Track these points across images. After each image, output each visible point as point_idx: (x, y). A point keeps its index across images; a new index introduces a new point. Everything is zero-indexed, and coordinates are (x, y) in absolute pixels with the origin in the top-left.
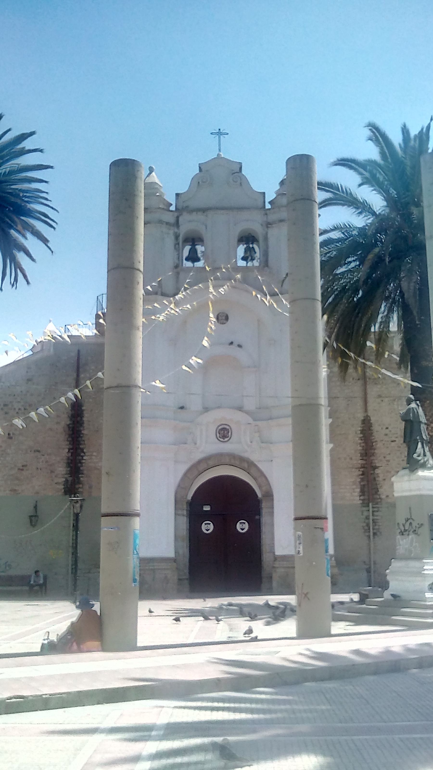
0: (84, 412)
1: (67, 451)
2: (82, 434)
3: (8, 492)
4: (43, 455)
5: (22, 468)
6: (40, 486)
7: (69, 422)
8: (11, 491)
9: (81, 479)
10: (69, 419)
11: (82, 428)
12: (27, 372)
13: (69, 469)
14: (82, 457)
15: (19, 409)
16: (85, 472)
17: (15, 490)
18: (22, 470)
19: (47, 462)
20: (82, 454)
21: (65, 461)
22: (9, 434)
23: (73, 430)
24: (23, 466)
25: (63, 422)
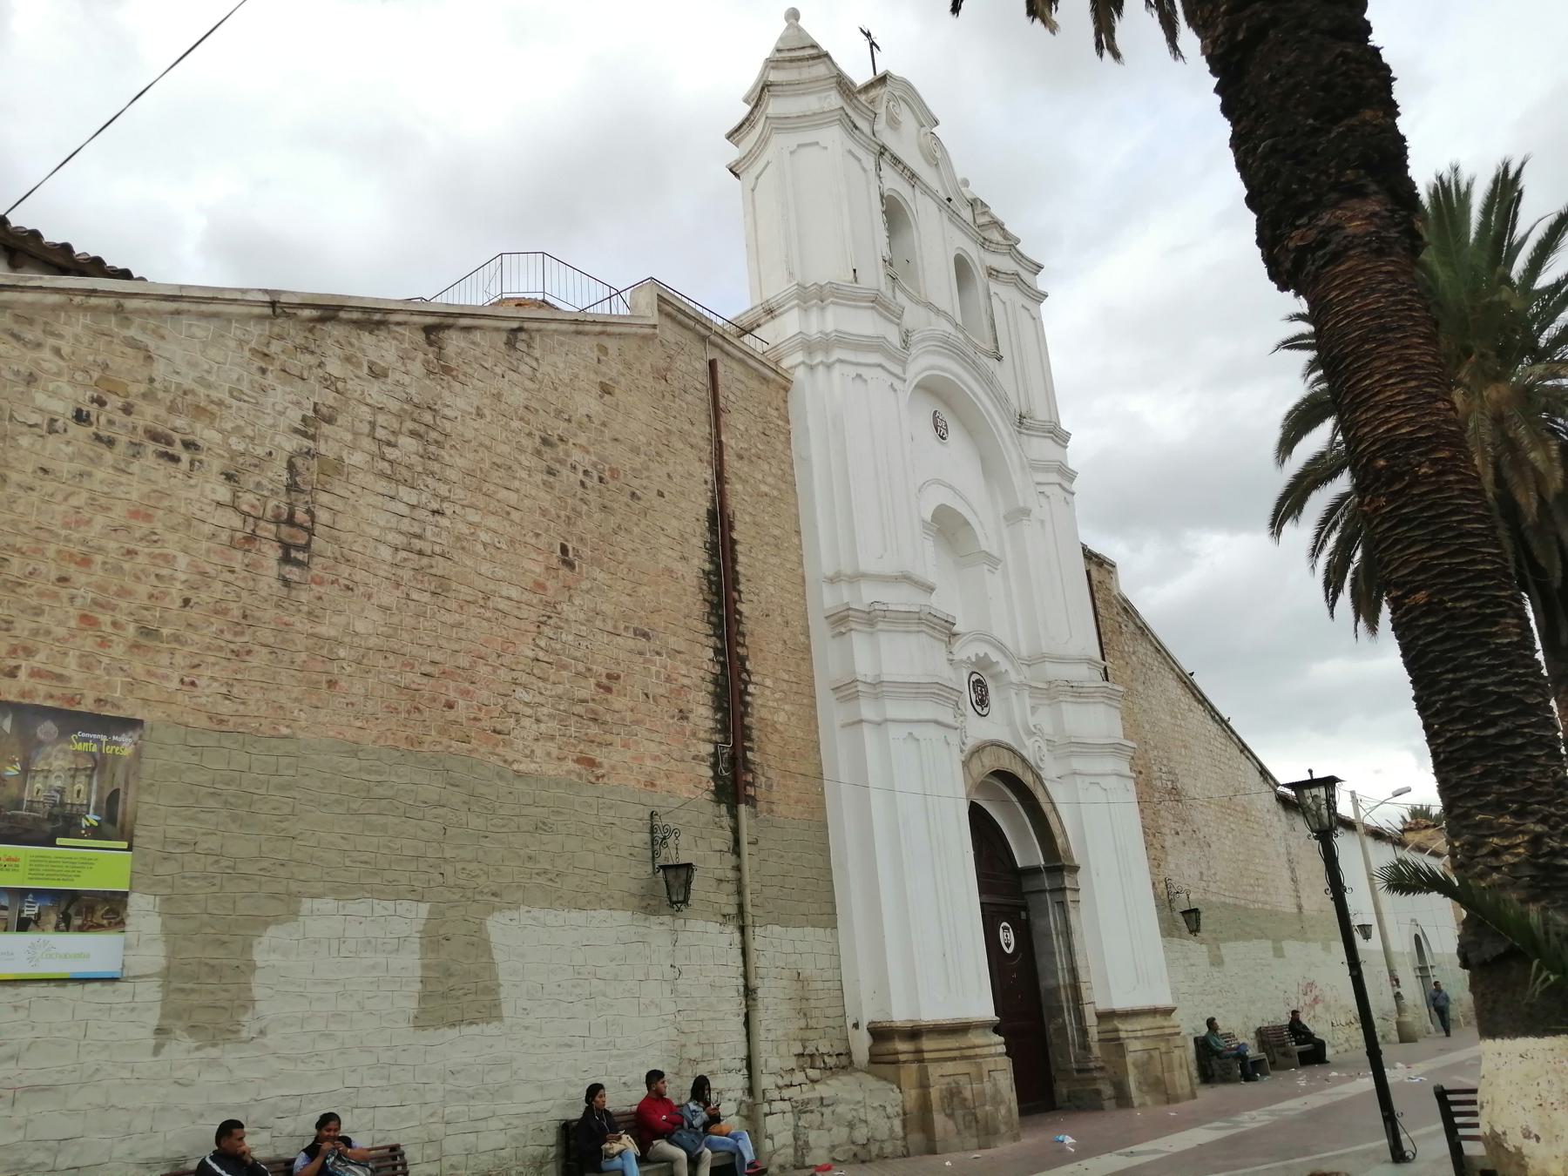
0: (738, 548)
1: (711, 654)
2: (740, 613)
3: (571, 765)
4: (658, 654)
5: (604, 681)
6: (655, 758)
7: (707, 567)
8: (578, 761)
9: (749, 754)
10: (706, 556)
11: (736, 595)
13: (718, 716)
14: (746, 683)
15: (586, 472)
16: (755, 734)
17: (591, 763)
18: (608, 690)
19: (668, 679)
20: (744, 676)
21: (711, 688)
22: (564, 550)
23: (718, 594)
24: (609, 676)
25: (696, 562)
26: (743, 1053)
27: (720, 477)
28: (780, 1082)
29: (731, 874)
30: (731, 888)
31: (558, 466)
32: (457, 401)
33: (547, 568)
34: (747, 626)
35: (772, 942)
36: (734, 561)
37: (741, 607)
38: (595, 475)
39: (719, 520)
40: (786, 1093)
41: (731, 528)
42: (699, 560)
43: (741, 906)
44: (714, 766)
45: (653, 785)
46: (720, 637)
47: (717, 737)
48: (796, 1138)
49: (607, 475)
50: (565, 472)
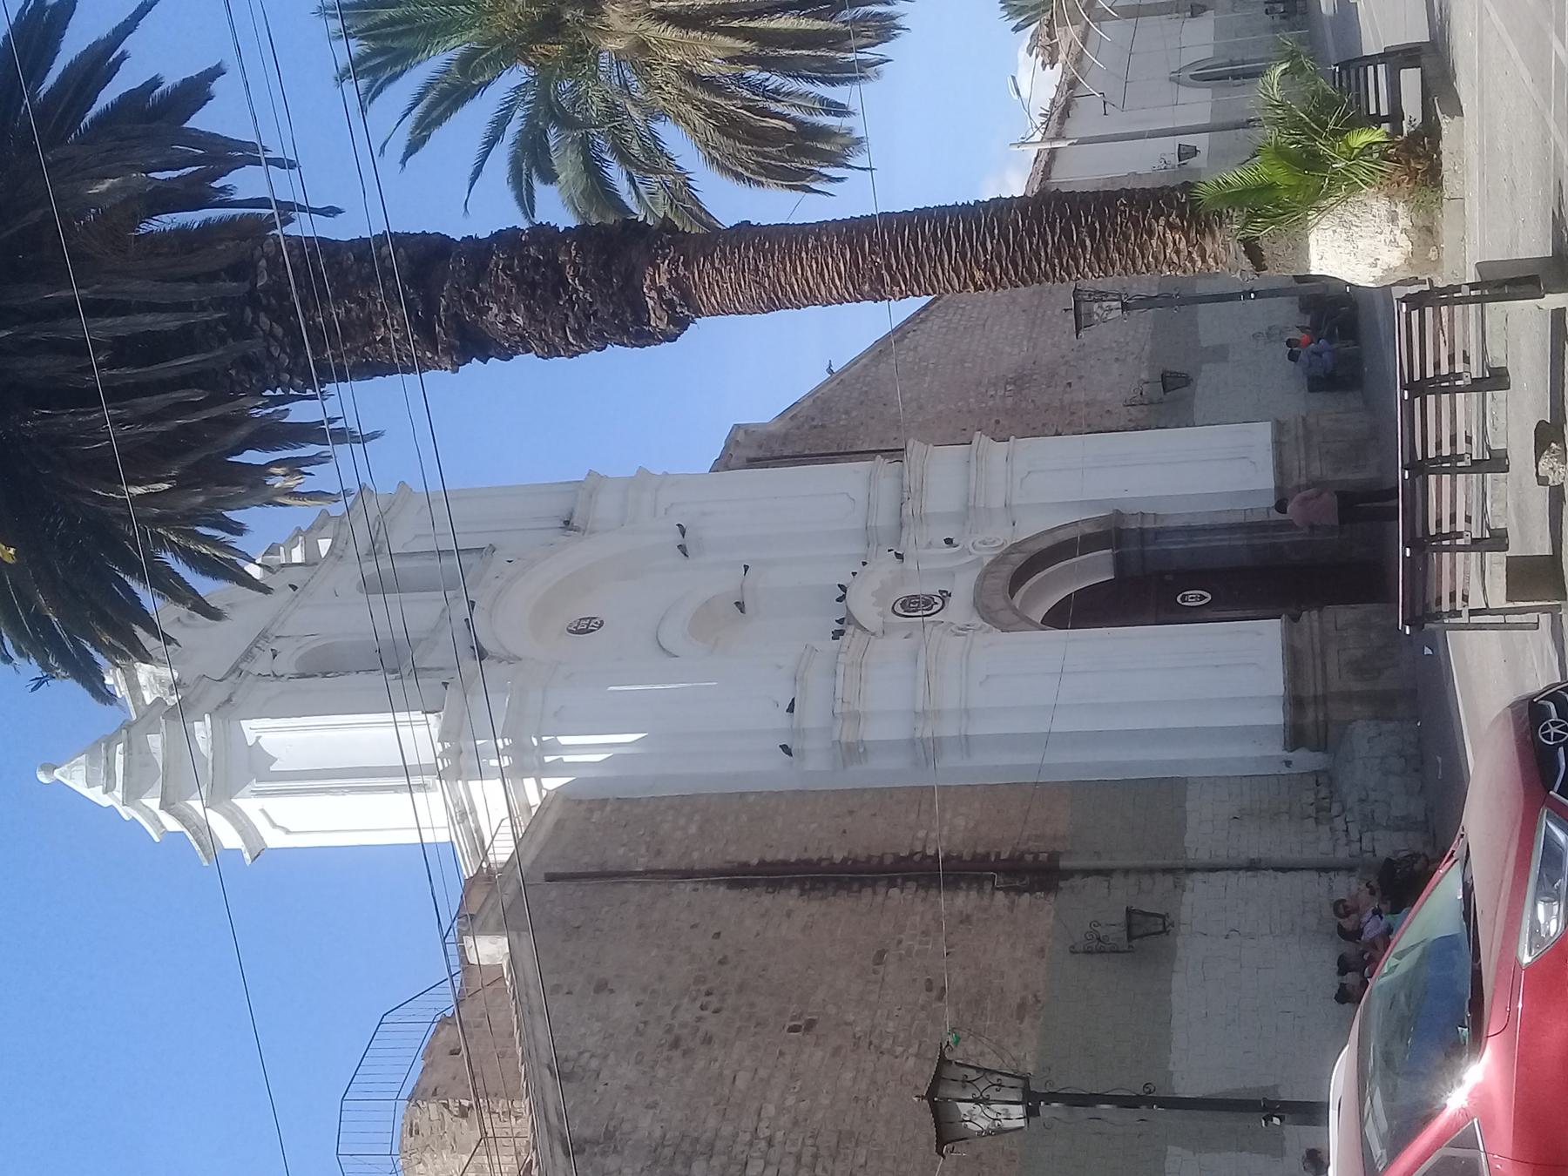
0: (768, 858)
1: (894, 892)
2: (845, 860)
4: (900, 942)
5: (934, 994)
6: (1013, 946)
7: (795, 891)
12: (569, 993)
13: (963, 885)
14: (925, 857)
15: (703, 1008)
16: (981, 850)
20: (917, 858)
21: (933, 892)
23: (825, 881)
24: (929, 989)
26: (1315, 875)
27: (688, 874)
28: (1343, 841)
29: (1132, 879)
30: (1146, 881)
31: (700, 1034)
32: (647, 1125)
33: (816, 1045)
34: (861, 853)
35: (1200, 841)
36: (785, 863)
37: (838, 857)
38: (703, 999)
39: (740, 877)
40: (1355, 835)
41: (746, 864)
42: (790, 899)
43: (1167, 871)
44: (1020, 891)
45: (1042, 950)
46: (875, 881)
47: (988, 887)
48: (1398, 829)
49: (704, 988)
50: (704, 1027)
